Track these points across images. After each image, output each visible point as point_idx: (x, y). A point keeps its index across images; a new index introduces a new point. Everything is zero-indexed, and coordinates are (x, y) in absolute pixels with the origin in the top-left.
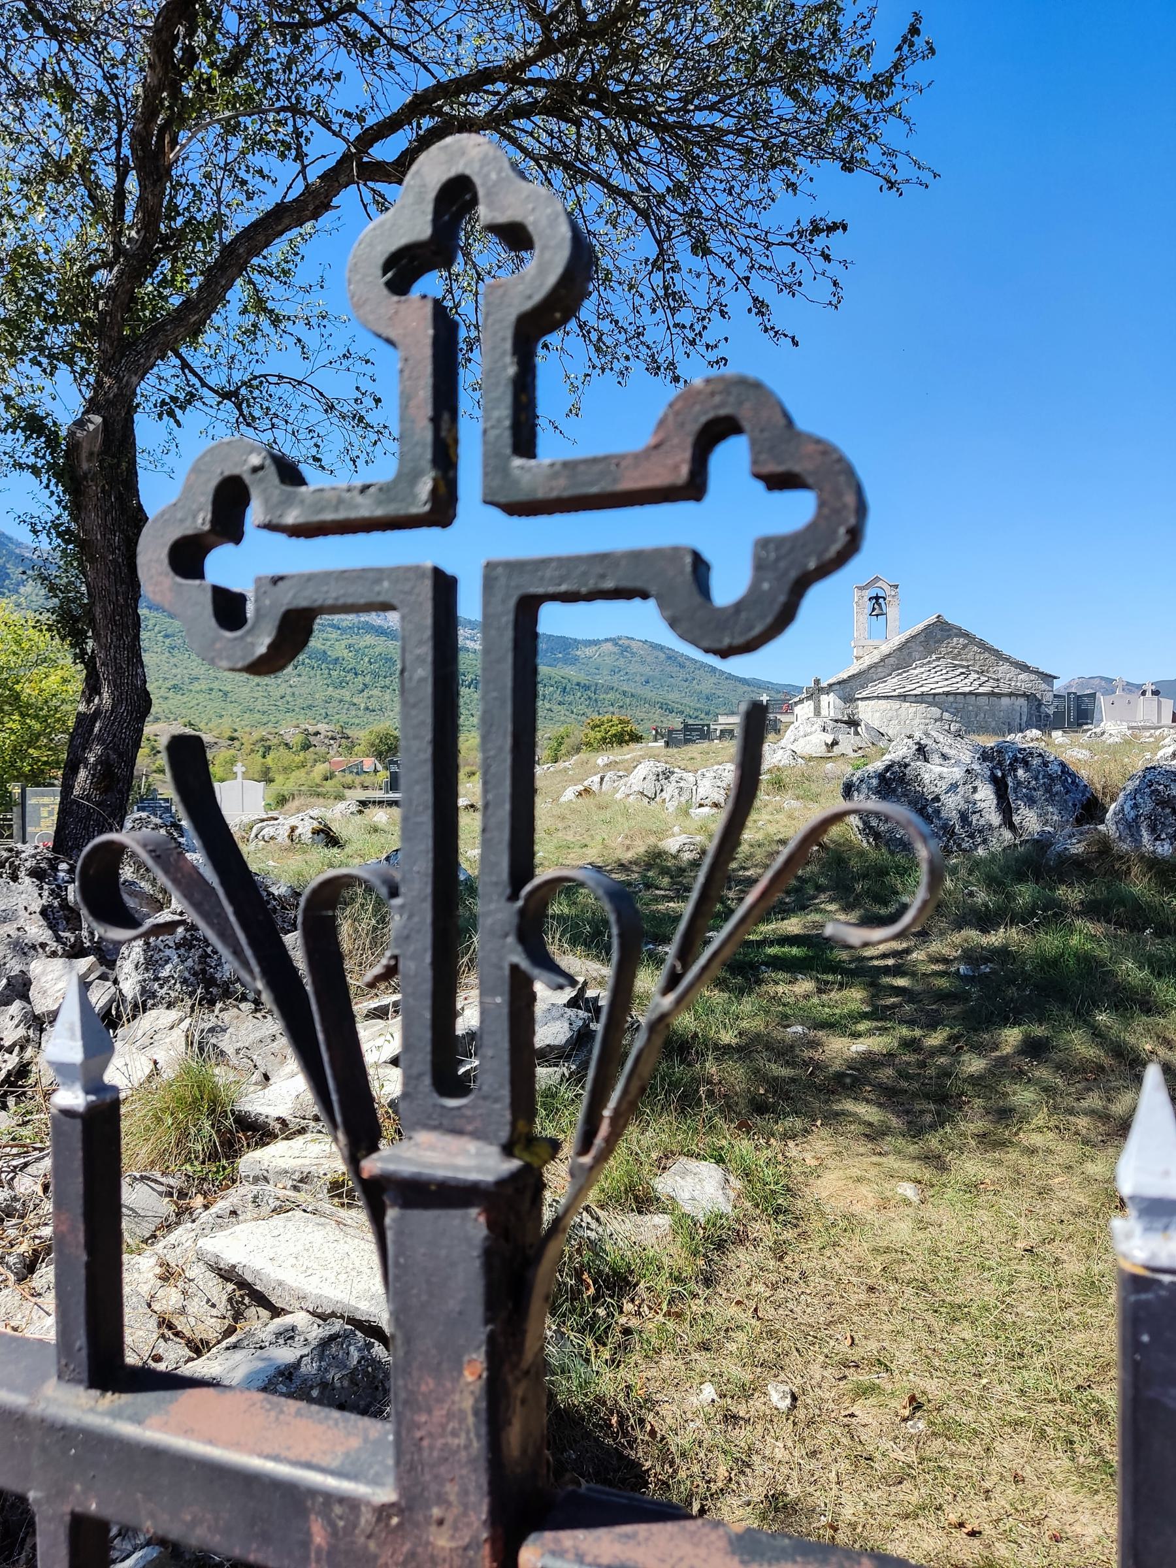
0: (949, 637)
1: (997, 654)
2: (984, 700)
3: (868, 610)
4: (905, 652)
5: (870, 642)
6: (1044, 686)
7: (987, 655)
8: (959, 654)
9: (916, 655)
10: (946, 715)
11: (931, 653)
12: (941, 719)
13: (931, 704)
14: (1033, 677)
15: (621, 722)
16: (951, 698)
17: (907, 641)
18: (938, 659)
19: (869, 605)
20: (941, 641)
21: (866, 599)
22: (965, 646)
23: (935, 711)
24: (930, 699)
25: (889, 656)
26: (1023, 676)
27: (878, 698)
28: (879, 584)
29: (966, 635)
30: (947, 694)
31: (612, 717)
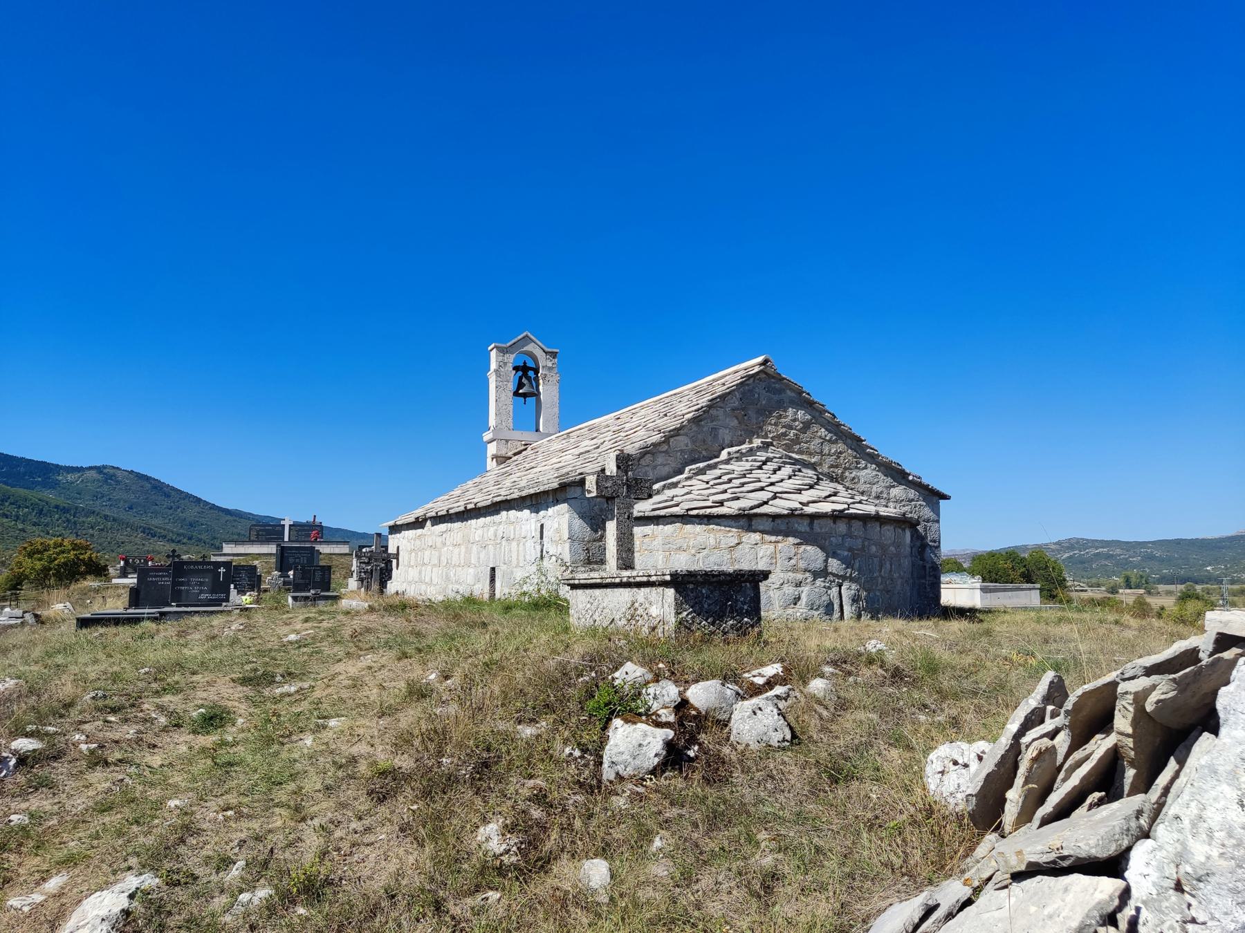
0: (781, 406)
1: (855, 443)
2: (888, 531)
3: (511, 387)
4: (707, 426)
5: (517, 435)
6: (927, 512)
7: (841, 446)
8: (796, 441)
9: (725, 435)
10: (835, 565)
11: (750, 434)
12: (823, 573)
13: (807, 539)
14: (912, 493)
15: (75, 547)
16: (842, 527)
17: (713, 404)
18: (766, 446)
19: (512, 377)
20: (765, 412)
21: (510, 367)
22: (806, 426)
23: (813, 554)
24: (803, 526)
25: (677, 432)
26: (898, 491)
27: (685, 518)
28: (530, 348)
29: (809, 405)
30: (836, 516)
31: (61, 542)
